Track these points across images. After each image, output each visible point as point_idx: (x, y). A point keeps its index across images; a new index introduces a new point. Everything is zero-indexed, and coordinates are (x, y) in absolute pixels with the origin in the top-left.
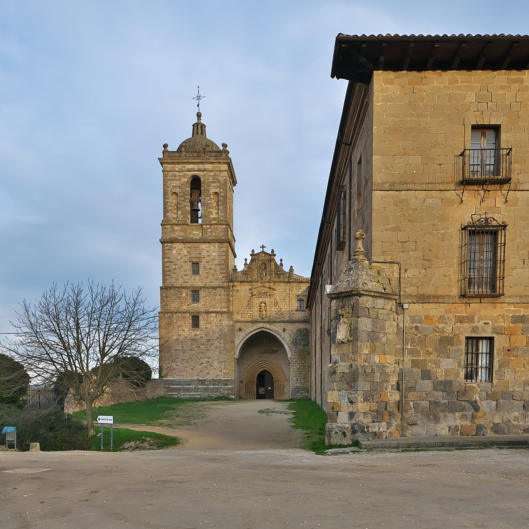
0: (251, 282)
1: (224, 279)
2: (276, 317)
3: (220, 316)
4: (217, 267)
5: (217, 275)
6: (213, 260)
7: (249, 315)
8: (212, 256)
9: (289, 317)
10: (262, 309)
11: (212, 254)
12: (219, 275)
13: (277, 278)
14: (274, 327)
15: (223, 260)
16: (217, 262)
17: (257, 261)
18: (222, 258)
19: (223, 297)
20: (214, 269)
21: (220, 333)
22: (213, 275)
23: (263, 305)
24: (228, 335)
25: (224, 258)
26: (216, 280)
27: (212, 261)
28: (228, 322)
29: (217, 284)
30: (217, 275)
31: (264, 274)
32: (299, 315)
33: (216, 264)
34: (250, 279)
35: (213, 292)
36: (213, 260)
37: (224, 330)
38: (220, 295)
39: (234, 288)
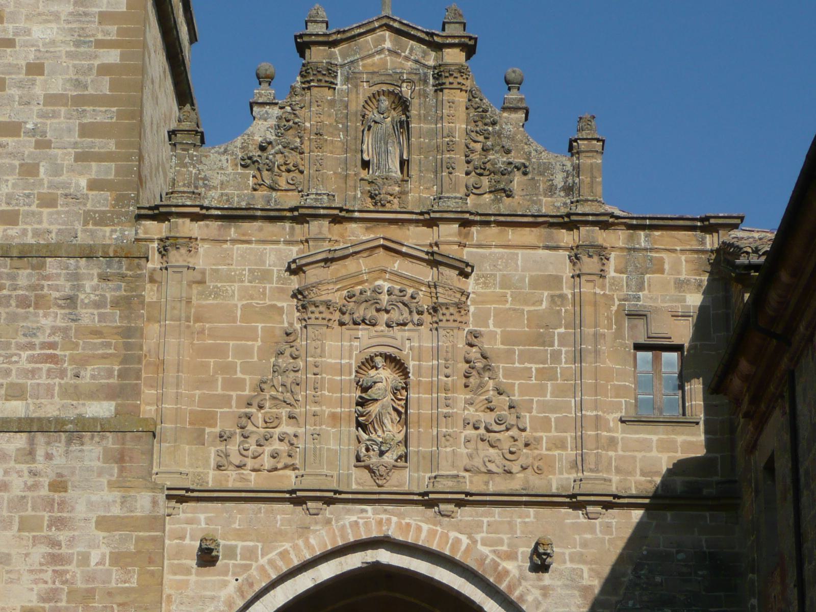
0: (300, 216)
1: (102, 201)
2: (477, 462)
3: (58, 449)
4: (55, 115)
5: (56, 170)
6: (35, 69)
7: (277, 445)
8: (26, 45)
9: (574, 466)
10: (374, 409)
11: (28, 32)
12: (71, 170)
13: (488, 197)
14: (465, 540)
15: (104, 70)
16: (57, 85)
17: (347, 79)
18: (96, 57)
19: (88, 317)
20: (33, 132)
21: (48, 576)
22: (29, 170)
23: (385, 376)
24: (110, 594)
25: (112, 56)
26: (48, 201)
27: (22, 76)
28: (117, 494)
29: (54, 228)
30: (56, 170)
31: (395, 165)
32: (654, 453)
33: (52, 99)
34: (291, 200)
35: (22, 281)
36: (35, 69)
37: (84, 559)
38: (71, 301)
39: (177, 257)
